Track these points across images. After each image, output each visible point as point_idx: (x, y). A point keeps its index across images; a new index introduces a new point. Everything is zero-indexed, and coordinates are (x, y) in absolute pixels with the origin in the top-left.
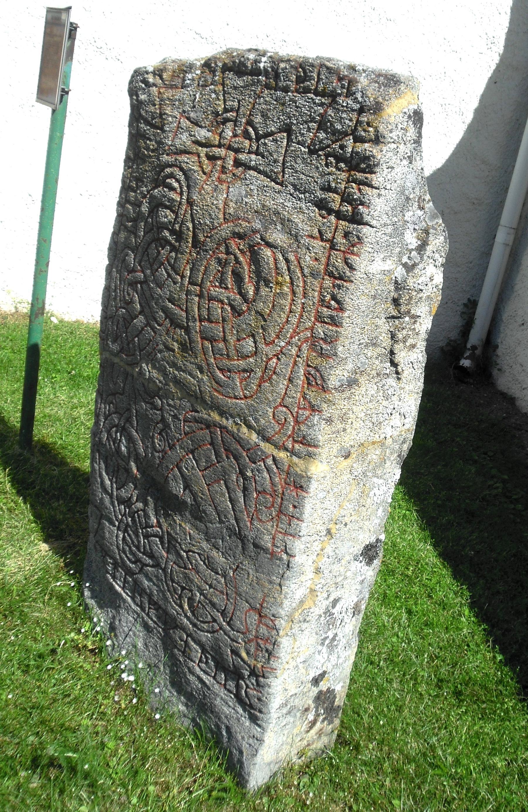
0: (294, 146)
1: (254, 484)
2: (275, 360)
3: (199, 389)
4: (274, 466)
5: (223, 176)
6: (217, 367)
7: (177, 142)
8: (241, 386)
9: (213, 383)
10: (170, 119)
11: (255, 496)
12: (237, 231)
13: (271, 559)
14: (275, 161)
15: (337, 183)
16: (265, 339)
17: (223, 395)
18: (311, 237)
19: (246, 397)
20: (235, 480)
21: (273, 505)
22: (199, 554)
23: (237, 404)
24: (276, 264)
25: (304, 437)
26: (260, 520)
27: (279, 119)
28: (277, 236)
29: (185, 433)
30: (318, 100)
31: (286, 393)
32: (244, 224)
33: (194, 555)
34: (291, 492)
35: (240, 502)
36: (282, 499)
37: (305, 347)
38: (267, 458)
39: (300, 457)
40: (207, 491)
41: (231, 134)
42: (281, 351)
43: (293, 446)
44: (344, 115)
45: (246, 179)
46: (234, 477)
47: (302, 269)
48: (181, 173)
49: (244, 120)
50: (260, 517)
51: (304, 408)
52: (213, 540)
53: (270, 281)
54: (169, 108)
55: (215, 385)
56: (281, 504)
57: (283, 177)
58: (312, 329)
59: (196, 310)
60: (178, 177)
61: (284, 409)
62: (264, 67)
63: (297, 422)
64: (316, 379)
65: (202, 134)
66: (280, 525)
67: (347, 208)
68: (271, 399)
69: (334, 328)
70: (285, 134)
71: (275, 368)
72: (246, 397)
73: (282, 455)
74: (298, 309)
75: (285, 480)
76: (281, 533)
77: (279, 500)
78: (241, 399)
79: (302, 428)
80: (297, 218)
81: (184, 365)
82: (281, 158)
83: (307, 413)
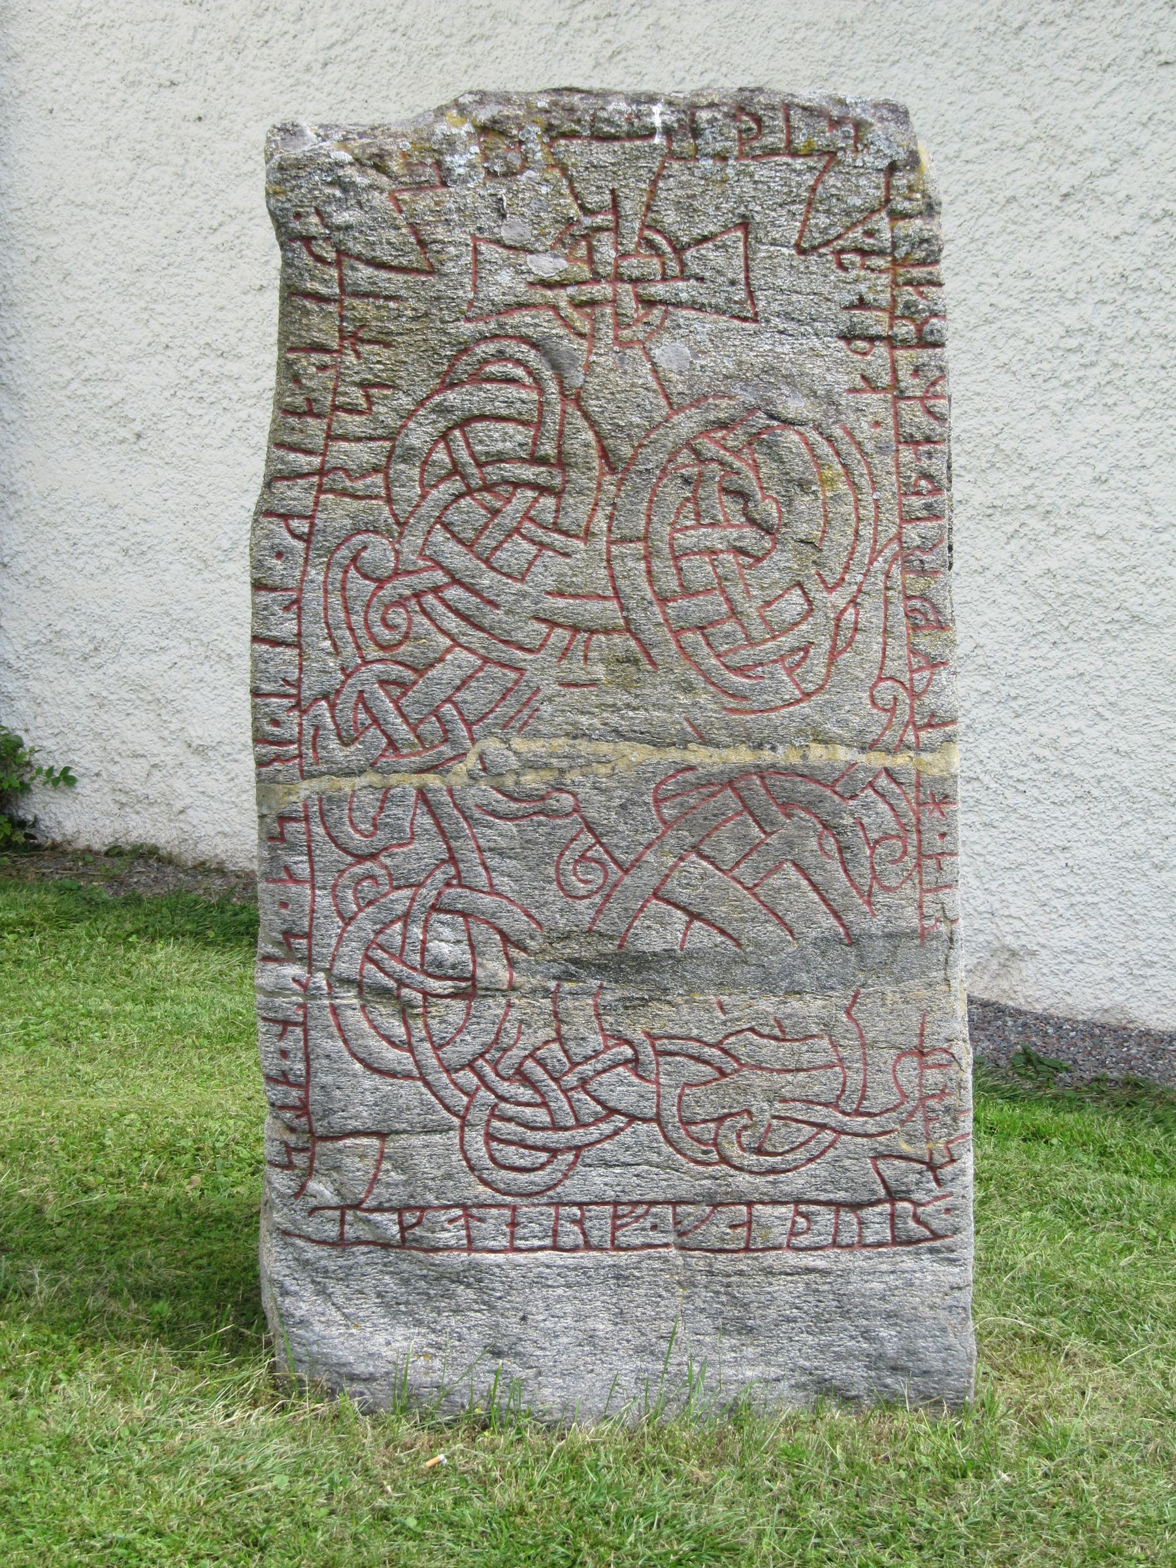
0: (763, 251)
1: (861, 834)
2: (851, 610)
3: (691, 725)
4: (893, 785)
5: (626, 333)
6: (727, 667)
7: (494, 292)
8: (793, 680)
9: (725, 699)
10: (452, 249)
11: (868, 853)
12: (712, 418)
13: (922, 945)
14: (733, 283)
15: (877, 292)
16: (823, 582)
17: (754, 712)
18: (853, 390)
19: (808, 695)
20: (816, 847)
21: (905, 853)
22: (752, 1030)
23: (791, 714)
24: (812, 450)
25: (933, 715)
26: (888, 889)
27: (718, 208)
28: (795, 406)
29: (664, 822)
30: (798, 163)
31: (884, 656)
32: (724, 403)
33: (741, 1037)
34: (930, 817)
35: (838, 880)
36: (919, 832)
37: (896, 571)
38: (876, 777)
39: (933, 751)
40: (753, 900)
41: (613, 254)
42: (859, 591)
43: (917, 737)
44: (863, 182)
45: (679, 326)
46: (813, 843)
47: (859, 445)
48: (524, 347)
49: (637, 225)
50: (886, 883)
51: (920, 669)
52: (784, 984)
53: (810, 482)
54: (440, 230)
55: (732, 703)
56: (920, 841)
57: (754, 305)
58: (899, 537)
59: (646, 585)
60: (519, 356)
61: (889, 683)
62: (663, 122)
63: (914, 695)
64: (925, 614)
65: (546, 265)
66: (925, 879)
67: (905, 329)
68: (863, 676)
69: (934, 523)
70: (739, 234)
71: (856, 623)
72: (809, 695)
73: (901, 760)
74: (868, 512)
75: (917, 798)
76: (929, 891)
77: (914, 836)
78: (798, 701)
79: (927, 701)
80: (815, 368)
81: (637, 696)
82: (742, 276)
83: (926, 674)
